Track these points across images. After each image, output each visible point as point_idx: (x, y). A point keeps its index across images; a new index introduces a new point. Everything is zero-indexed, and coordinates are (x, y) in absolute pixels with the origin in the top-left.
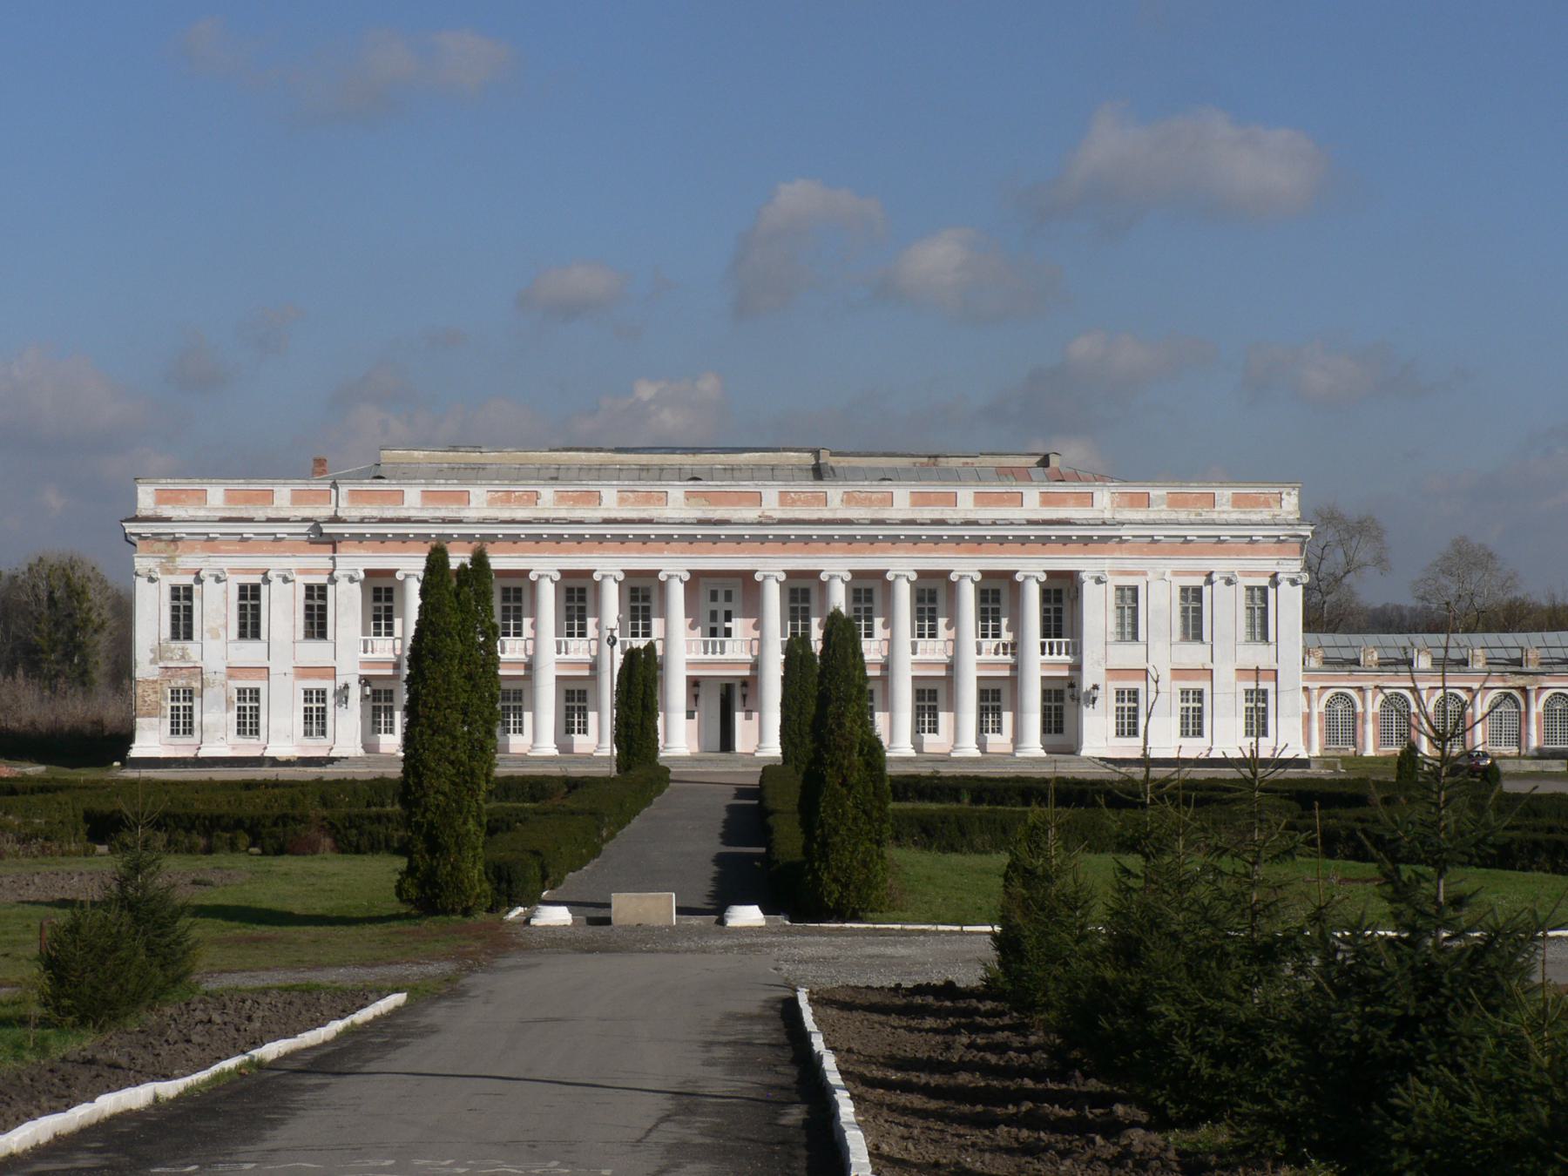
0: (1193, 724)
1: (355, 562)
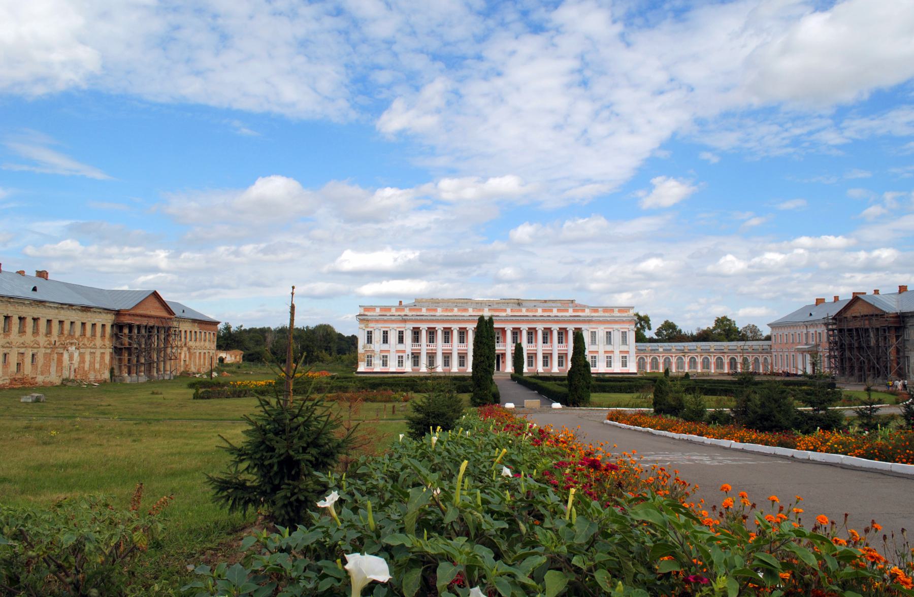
0: (609, 364)
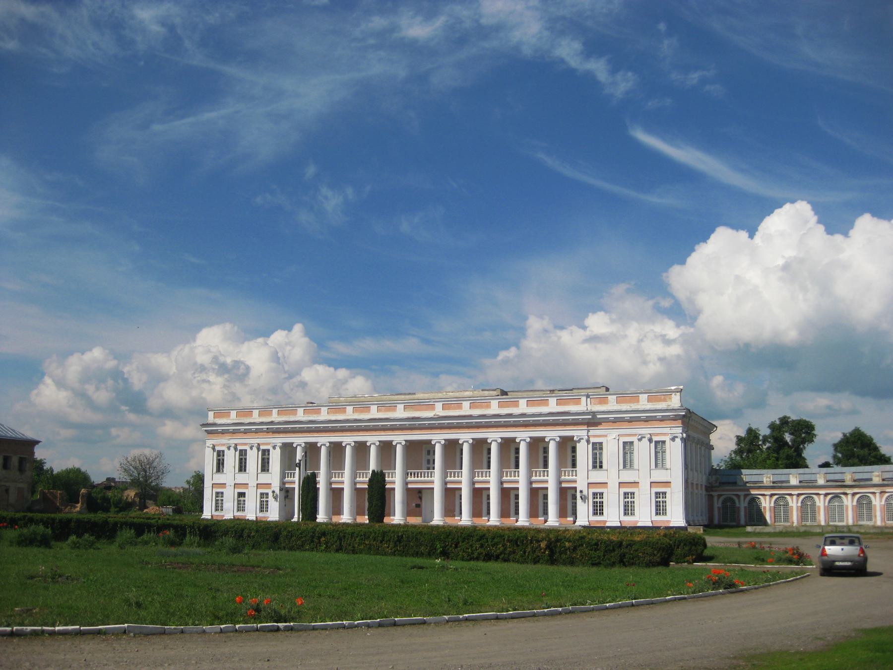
0: (628, 509)
1: (280, 440)
